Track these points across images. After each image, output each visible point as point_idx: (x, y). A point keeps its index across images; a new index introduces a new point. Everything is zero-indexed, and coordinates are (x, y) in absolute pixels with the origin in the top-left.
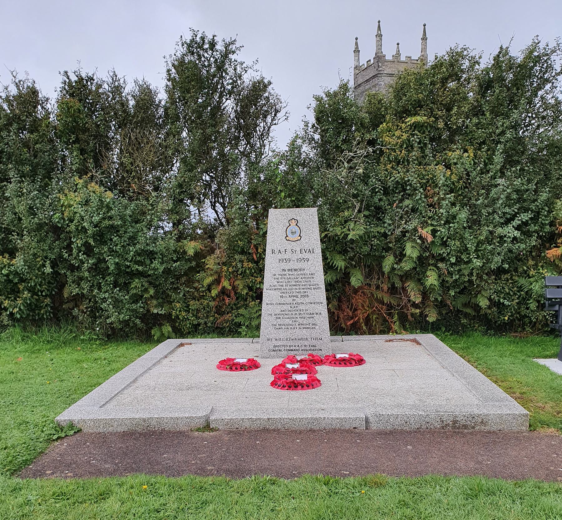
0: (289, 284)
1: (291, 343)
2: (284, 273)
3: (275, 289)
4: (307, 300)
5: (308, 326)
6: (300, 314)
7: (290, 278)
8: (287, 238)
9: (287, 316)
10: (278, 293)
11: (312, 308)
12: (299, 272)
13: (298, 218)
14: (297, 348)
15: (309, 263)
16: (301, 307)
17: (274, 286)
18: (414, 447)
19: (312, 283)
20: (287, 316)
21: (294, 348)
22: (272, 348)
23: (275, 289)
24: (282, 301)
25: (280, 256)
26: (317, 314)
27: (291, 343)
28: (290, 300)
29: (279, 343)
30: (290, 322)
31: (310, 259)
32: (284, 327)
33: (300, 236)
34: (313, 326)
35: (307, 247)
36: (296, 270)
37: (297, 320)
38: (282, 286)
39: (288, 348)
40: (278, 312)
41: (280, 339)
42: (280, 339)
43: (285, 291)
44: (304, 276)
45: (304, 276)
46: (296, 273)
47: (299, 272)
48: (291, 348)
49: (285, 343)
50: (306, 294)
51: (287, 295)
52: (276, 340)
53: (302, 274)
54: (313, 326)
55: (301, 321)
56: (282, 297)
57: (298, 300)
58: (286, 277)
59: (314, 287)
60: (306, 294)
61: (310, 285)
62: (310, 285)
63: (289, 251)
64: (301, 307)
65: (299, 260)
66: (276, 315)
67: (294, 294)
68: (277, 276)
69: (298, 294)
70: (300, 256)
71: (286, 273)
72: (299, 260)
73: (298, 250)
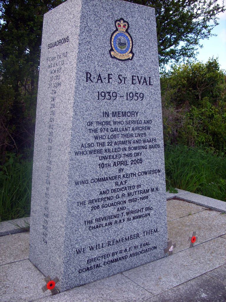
0: (114, 140)
1: (115, 248)
2: (105, 119)
3: (91, 152)
4: (141, 168)
5: (140, 214)
6: (129, 195)
7: (116, 130)
8: (112, 53)
9: (110, 202)
10: (95, 159)
11: (145, 182)
12: (130, 119)
13: (129, 20)
14: (124, 254)
15: (145, 102)
16: (133, 181)
17: (90, 145)
18: (214, 183)
19: (148, 138)
20: (110, 202)
21: (120, 255)
22: (84, 265)
23: (91, 152)
24: (103, 173)
25: (100, 87)
26: (152, 190)
27: (115, 248)
28: (113, 171)
29: (97, 253)
30: (115, 212)
31: (146, 95)
32: (104, 222)
33: (131, 52)
34: (147, 212)
35: (142, 73)
36: (124, 114)
37: (125, 205)
38: (103, 144)
39: (111, 258)
40: (95, 196)
41: (98, 246)
42: (98, 246)
43: (108, 154)
44: (136, 125)
45: (136, 125)
46: (124, 119)
47: (130, 119)
48: (115, 257)
49: (105, 251)
50: (139, 157)
51: (111, 161)
52: (92, 249)
53: (133, 122)
54: (147, 212)
55: (130, 206)
56: (102, 166)
57: (128, 169)
58: (109, 127)
59: (151, 144)
60: (139, 157)
61: (144, 142)
62: (144, 142)
63: (115, 77)
64: (133, 181)
65: (131, 96)
66: (91, 202)
67: (122, 159)
68: (95, 126)
69: (127, 158)
70: (132, 88)
71: (109, 119)
72: (131, 96)
73: (129, 76)
